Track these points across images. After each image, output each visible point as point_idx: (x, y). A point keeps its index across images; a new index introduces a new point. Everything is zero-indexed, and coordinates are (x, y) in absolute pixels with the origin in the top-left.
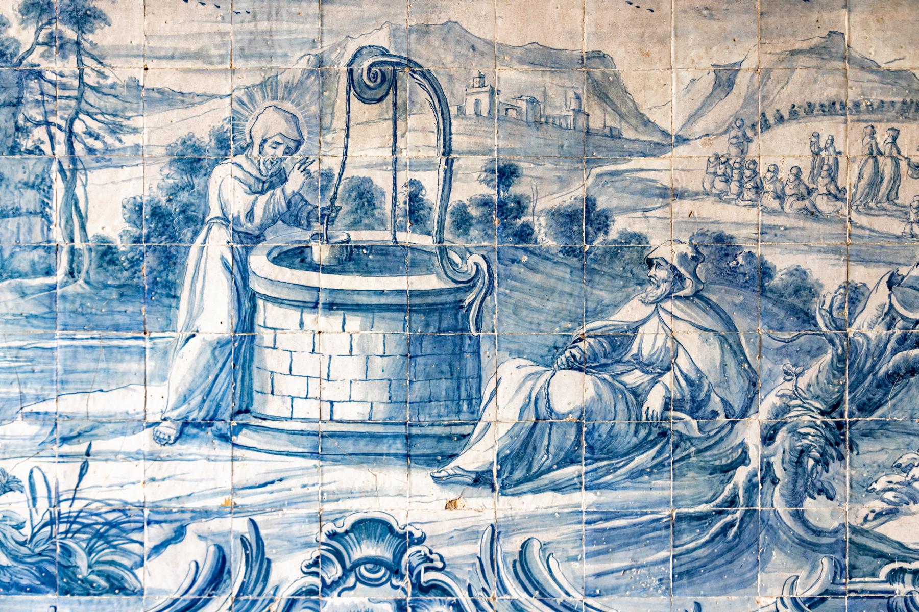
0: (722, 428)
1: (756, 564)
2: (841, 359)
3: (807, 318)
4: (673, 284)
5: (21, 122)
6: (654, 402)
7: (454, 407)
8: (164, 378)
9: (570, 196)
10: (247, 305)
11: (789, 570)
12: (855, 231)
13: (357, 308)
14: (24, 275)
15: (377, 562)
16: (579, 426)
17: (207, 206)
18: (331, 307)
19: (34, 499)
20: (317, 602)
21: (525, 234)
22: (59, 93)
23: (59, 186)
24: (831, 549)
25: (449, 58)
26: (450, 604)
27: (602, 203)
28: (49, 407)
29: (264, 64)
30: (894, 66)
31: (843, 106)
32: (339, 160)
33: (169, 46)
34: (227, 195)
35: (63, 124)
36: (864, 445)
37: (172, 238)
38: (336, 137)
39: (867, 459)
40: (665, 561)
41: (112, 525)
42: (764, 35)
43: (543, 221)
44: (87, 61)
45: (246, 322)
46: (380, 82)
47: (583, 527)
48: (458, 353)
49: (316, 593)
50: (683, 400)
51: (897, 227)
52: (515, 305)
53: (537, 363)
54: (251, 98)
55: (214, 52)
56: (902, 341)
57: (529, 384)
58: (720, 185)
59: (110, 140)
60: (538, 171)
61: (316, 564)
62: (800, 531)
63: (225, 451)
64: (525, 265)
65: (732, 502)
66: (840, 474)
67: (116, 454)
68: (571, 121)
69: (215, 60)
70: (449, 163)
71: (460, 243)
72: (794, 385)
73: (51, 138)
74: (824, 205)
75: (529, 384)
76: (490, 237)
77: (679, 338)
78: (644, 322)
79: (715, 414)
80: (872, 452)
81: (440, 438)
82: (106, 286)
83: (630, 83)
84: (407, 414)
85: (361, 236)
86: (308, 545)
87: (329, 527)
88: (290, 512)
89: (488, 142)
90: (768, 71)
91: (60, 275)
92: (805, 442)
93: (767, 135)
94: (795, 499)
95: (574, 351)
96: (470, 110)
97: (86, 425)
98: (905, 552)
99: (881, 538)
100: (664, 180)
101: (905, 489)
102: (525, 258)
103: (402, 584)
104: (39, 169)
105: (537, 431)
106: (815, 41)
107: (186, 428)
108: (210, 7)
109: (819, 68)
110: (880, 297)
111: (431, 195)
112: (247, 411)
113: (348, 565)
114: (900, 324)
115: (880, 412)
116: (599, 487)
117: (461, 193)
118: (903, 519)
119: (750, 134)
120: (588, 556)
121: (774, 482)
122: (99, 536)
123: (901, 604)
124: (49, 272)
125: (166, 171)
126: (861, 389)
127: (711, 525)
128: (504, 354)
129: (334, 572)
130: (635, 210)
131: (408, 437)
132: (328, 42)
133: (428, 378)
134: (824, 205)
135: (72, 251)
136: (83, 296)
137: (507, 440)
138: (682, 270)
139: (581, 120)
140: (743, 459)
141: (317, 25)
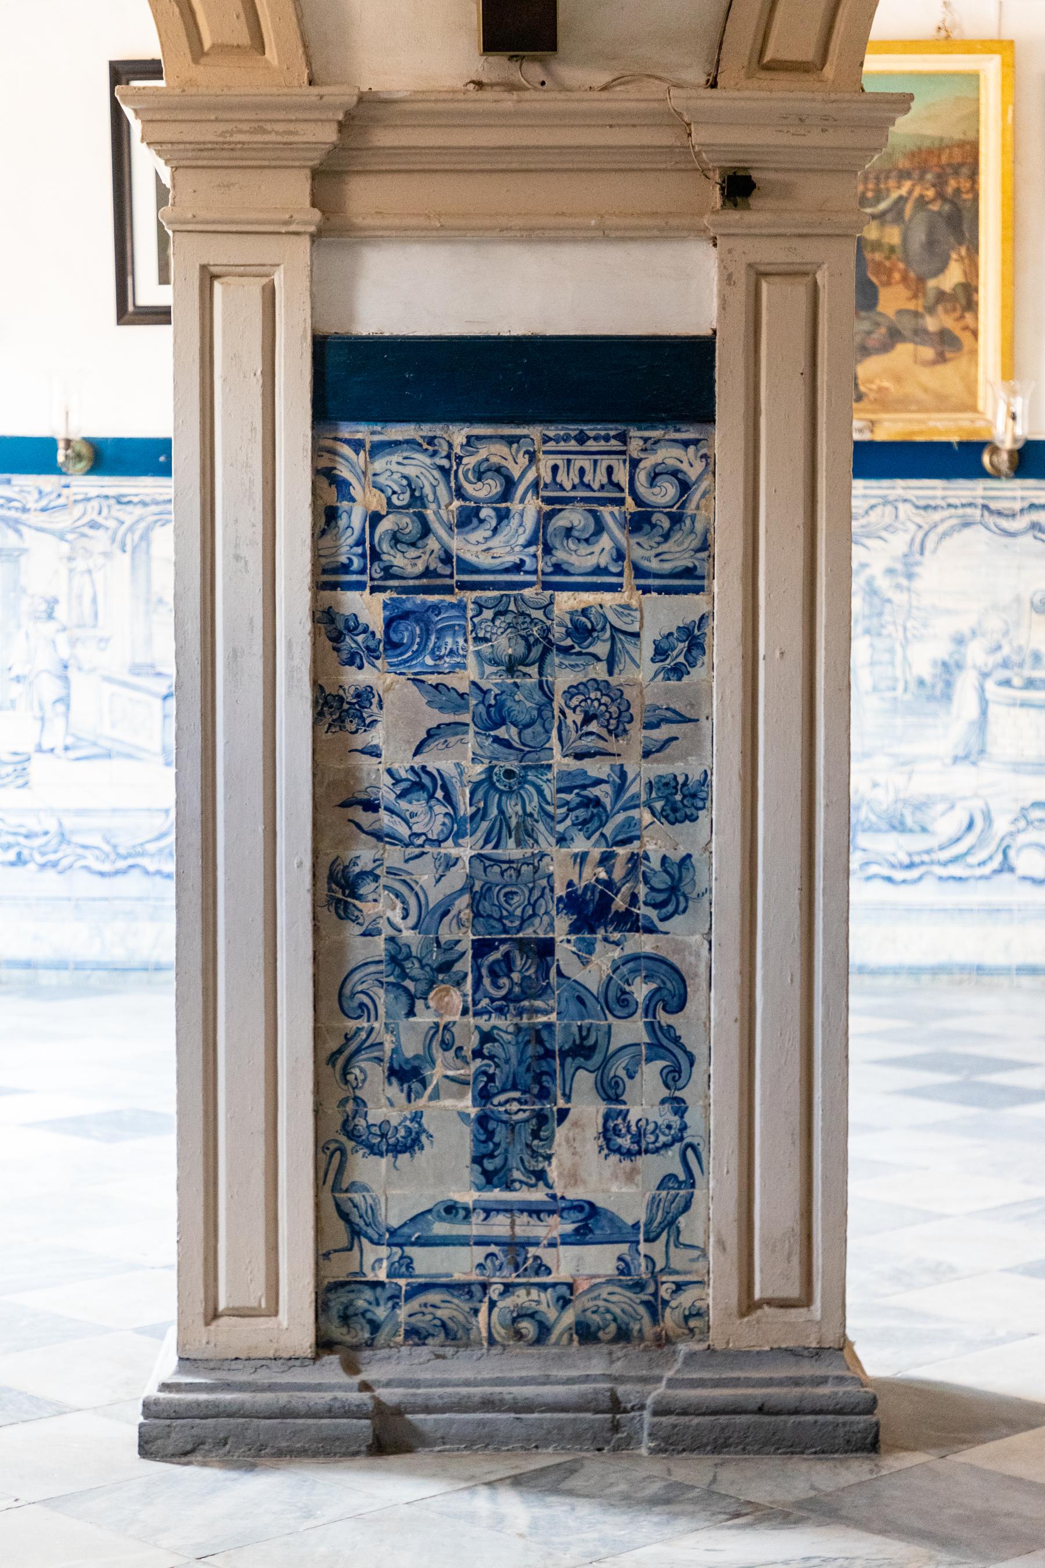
23: (899, 650)
45: (984, 712)
107: (956, 759)
129: (1022, 824)
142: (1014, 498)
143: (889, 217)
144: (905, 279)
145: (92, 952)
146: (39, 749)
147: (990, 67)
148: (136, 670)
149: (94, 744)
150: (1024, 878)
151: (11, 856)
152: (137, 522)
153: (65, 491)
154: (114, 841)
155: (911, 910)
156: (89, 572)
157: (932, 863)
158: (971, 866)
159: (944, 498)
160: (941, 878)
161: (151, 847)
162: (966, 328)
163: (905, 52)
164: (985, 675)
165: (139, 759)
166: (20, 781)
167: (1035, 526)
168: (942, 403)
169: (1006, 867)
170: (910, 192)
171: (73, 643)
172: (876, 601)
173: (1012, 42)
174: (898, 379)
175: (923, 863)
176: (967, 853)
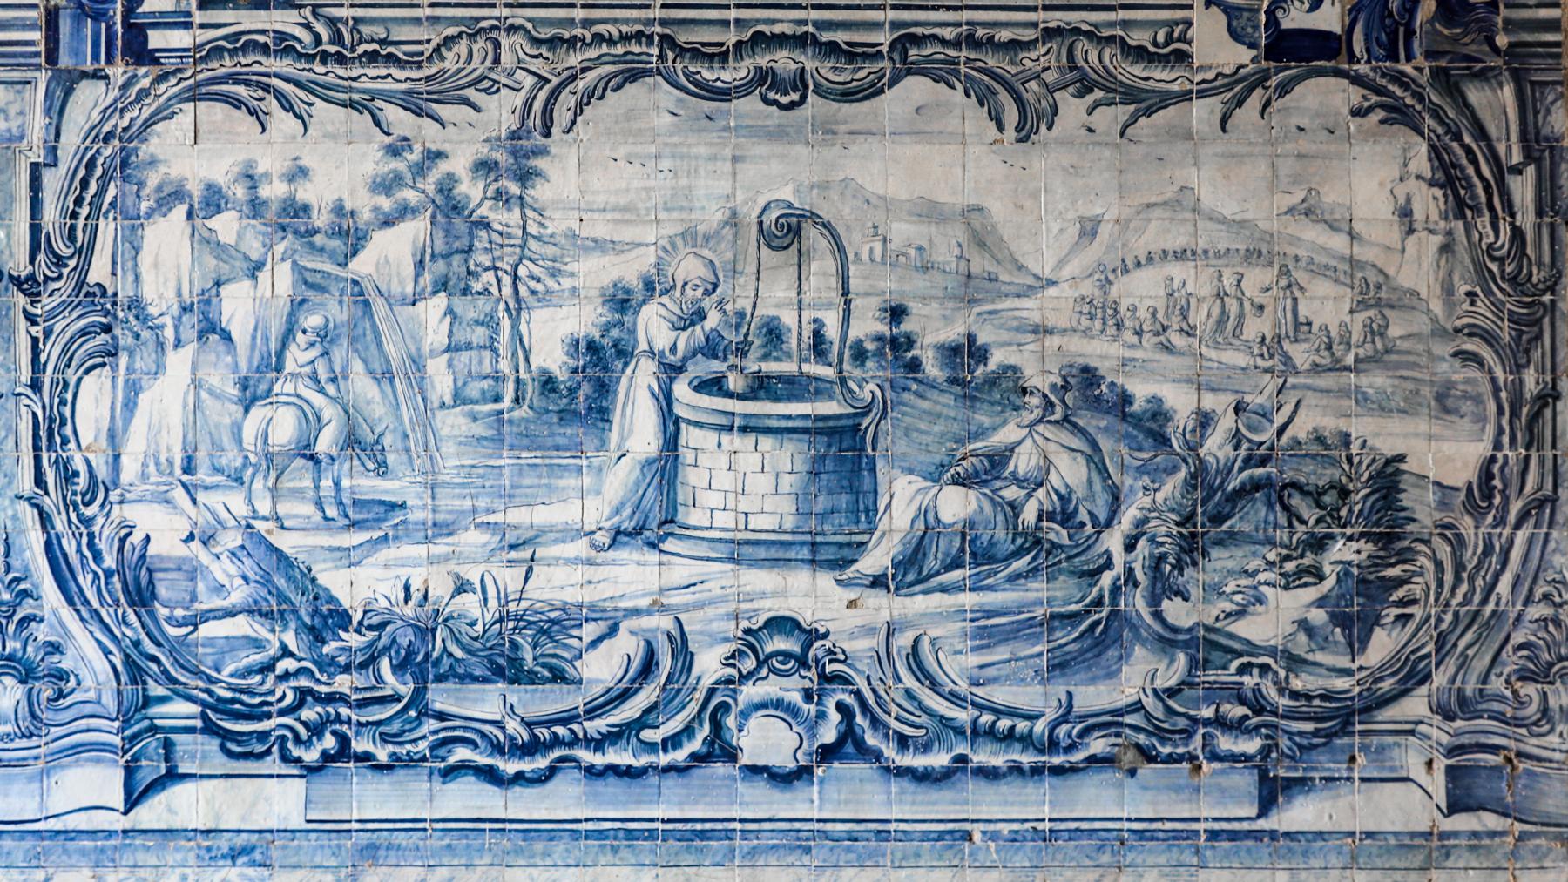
0: (1089, 537)
1: (1121, 658)
2: (1194, 476)
3: (1162, 441)
4: (1045, 410)
5: (472, 267)
6: (1029, 515)
7: (853, 517)
8: (598, 493)
9: (953, 333)
10: (671, 428)
11: (1149, 663)
12: (1205, 363)
13: (768, 431)
14: (477, 402)
15: (786, 655)
16: (963, 535)
17: (636, 340)
18: (744, 429)
19: (486, 600)
20: (734, 691)
21: (914, 366)
22: (506, 241)
24: (1186, 645)
25: (847, 210)
26: (851, 692)
27: (981, 339)
28: (498, 518)
29: (684, 215)
30: (1238, 217)
31: (1194, 253)
32: (751, 300)
33: (600, 200)
34: (653, 332)
35: (509, 269)
36: (1215, 553)
37: (605, 369)
38: (746, 282)
39: (1218, 565)
40: (1040, 654)
41: (554, 622)
42: (1122, 190)
43: (930, 353)
44: (530, 213)
45: (671, 443)
46: (787, 233)
47: (968, 624)
48: (856, 471)
49: (733, 682)
50: (1054, 512)
51: (1241, 359)
52: (907, 429)
53: (925, 479)
54: (674, 246)
55: (640, 205)
56: (1248, 462)
57: (919, 498)
58: (1085, 323)
59: (551, 283)
60: (926, 311)
61: (733, 656)
62: (1159, 628)
63: (653, 557)
64: (916, 393)
65: (1099, 602)
67: (557, 559)
68: (953, 266)
69: (643, 212)
70: (848, 303)
71: (857, 373)
72: (1153, 499)
73: (499, 281)
74: (1178, 340)
75: (919, 498)
76: (884, 369)
77: (1051, 457)
78: (1020, 443)
79: (1083, 524)
80: (1221, 559)
81: (840, 545)
82: (548, 411)
83: (1006, 233)
84: (813, 524)
86: (727, 640)
87: (744, 624)
88: (710, 611)
89: (882, 285)
90: (1128, 221)
92: (1163, 549)
93: (1125, 279)
94: (1154, 600)
95: (959, 469)
96: (865, 256)
97: (531, 534)
98: (1252, 648)
99: (1231, 636)
100: (1036, 318)
101: (1252, 592)
102: (915, 387)
103: (809, 674)
104: (488, 309)
105: (927, 540)
106: (1169, 195)
107: (618, 536)
108: (637, 165)
109: (1172, 219)
110: (1227, 422)
111: (832, 331)
112: (672, 521)
113: (762, 657)
114: (1245, 445)
115: (1228, 523)
116: (981, 589)
118: (1249, 618)
119: (1111, 277)
120: (972, 650)
121: (1136, 585)
122: (542, 632)
123: (1250, 694)
124: (497, 399)
125: (599, 310)
126: (1212, 503)
127: (1080, 623)
128: (896, 472)
129: (749, 664)
130: (1010, 344)
131: (813, 544)
132: (740, 197)
133: (830, 493)
134: (1178, 340)
135: (518, 381)
136: (527, 420)
137: (900, 548)
138: (1053, 398)
139: (963, 264)
140: (1108, 565)
141: (731, 182)
142: (726, 23)
150: (754, 770)
155: (533, 833)
157: (575, 741)
158: (651, 747)
159: (587, 23)
160: (590, 772)
164: (672, 370)
167: (764, 78)
169: (720, 750)
172: (460, 225)
175: (556, 741)
176: (640, 723)
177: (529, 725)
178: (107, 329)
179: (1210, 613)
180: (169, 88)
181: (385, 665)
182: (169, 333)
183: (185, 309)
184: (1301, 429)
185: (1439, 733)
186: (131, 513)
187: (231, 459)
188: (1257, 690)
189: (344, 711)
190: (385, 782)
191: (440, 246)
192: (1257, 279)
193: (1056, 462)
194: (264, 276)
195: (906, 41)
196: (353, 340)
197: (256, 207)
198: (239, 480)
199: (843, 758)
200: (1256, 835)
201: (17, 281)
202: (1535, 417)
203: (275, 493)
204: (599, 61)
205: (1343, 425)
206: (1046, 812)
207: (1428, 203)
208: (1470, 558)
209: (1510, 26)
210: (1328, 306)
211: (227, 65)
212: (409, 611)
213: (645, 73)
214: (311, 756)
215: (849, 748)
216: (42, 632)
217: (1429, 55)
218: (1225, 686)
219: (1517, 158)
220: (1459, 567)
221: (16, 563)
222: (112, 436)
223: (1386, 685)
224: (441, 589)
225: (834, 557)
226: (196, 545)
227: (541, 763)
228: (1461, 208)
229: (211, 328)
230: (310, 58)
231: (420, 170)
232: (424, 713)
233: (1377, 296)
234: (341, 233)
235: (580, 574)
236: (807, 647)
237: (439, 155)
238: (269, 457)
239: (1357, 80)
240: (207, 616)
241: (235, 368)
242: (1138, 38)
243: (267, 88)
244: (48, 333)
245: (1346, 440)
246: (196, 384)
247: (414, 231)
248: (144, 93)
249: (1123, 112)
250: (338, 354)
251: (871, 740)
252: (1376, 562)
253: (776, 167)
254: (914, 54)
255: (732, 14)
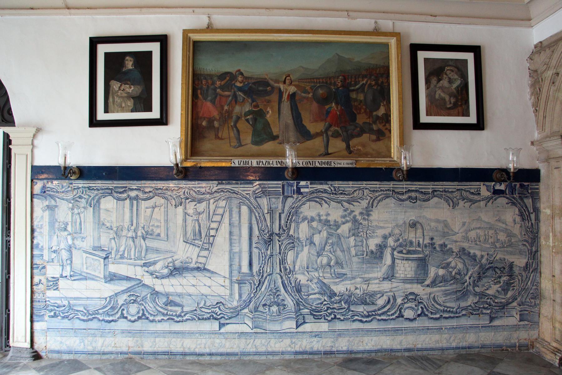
3: (475, 260)
6: (453, 273)
9: (441, 242)
13: (410, 260)
15: (412, 299)
18: (406, 260)
21: (435, 248)
27: (446, 243)
36: (483, 279)
46: (413, 225)
51: (488, 246)
56: (489, 263)
63: (390, 282)
66: (480, 284)
72: (473, 270)
74: (478, 243)
80: (485, 280)
85: (411, 249)
88: (400, 292)
91: (365, 255)
94: (473, 287)
98: (489, 295)
100: (455, 239)
107: (384, 279)
110: (486, 257)
111: (421, 242)
117: (425, 242)
129: (406, 301)
134: (478, 243)
140: (466, 282)
143: (359, 91)
144: (365, 112)
145: (81, 348)
146: (62, 276)
147: (393, 42)
148: (95, 248)
149: (81, 275)
150: (407, 319)
151: (52, 314)
152: (95, 196)
153: (71, 185)
154: (88, 309)
155: (369, 331)
156: (79, 214)
157: (376, 315)
158: (389, 315)
159: (379, 188)
160: (378, 320)
161: (101, 311)
162: (386, 129)
163: (364, 35)
165: (97, 280)
166: (55, 288)
167: (410, 197)
168: (379, 155)
170: (367, 82)
171: (73, 239)
172: (357, 224)
173: (400, 33)
174: (364, 146)
175: (373, 315)
177: (368, 312)
178: (293, 243)
179: (482, 289)
180: (304, 199)
181: (343, 302)
182: (304, 244)
183: (307, 239)
184: (497, 258)
185: (518, 308)
186: (297, 276)
187: (315, 266)
188: (490, 302)
189: (335, 311)
190: (343, 323)
191: (353, 228)
192: (491, 232)
193: (457, 264)
194: (321, 233)
195: (434, 191)
196: (337, 245)
197: (320, 221)
198: (317, 270)
199: (422, 316)
200: (489, 326)
201: (276, 234)
202: (534, 255)
203: (323, 272)
204: (381, 195)
205: (504, 257)
206: (455, 324)
207: (518, 219)
208: (524, 279)
209: (531, 189)
210: (502, 237)
211: (315, 195)
212: (347, 293)
213: (389, 197)
214: (329, 319)
215: (423, 314)
216: (281, 297)
217: (519, 194)
218: (484, 302)
219: (532, 211)
220: (522, 280)
221: (276, 285)
222: (294, 262)
223: (510, 300)
224: (353, 289)
225: (420, 281)
226: (309, 282)
227: (370, 319)
228: (523, 219)
229: (312, 243)
230: (330, 194)
231: (350, 214)
232: (349, 311)
233: (510, 235)
234: (336, 225)
235: (377, 286)
236: (416, 298)
237: (353, 211)
238: (322, 266)
239: (507, 198)
240: (311, 294)
241: (316, 250)
242: (472, 191)
243: (322, 199)
244: (282, 244)
245: (505, 259)
246: (309, 253)
247: (349, 225)
248: (300, 200)
249: (469, 204)
250: (335, 247)
251: (426, 313)
252: (509, 280)
253: (412, 213)
254: (435, 193)
255: (405, 186)
